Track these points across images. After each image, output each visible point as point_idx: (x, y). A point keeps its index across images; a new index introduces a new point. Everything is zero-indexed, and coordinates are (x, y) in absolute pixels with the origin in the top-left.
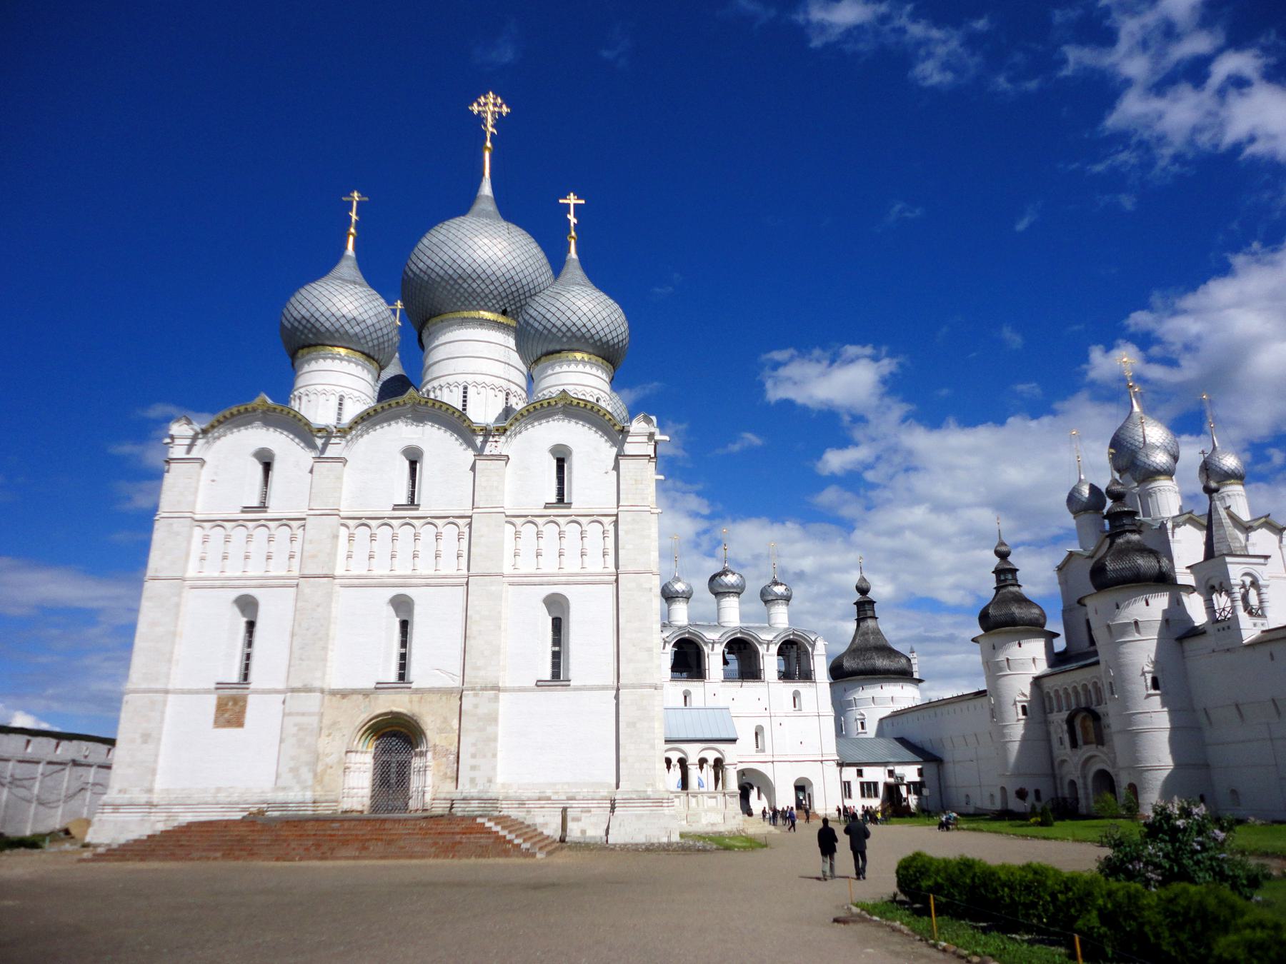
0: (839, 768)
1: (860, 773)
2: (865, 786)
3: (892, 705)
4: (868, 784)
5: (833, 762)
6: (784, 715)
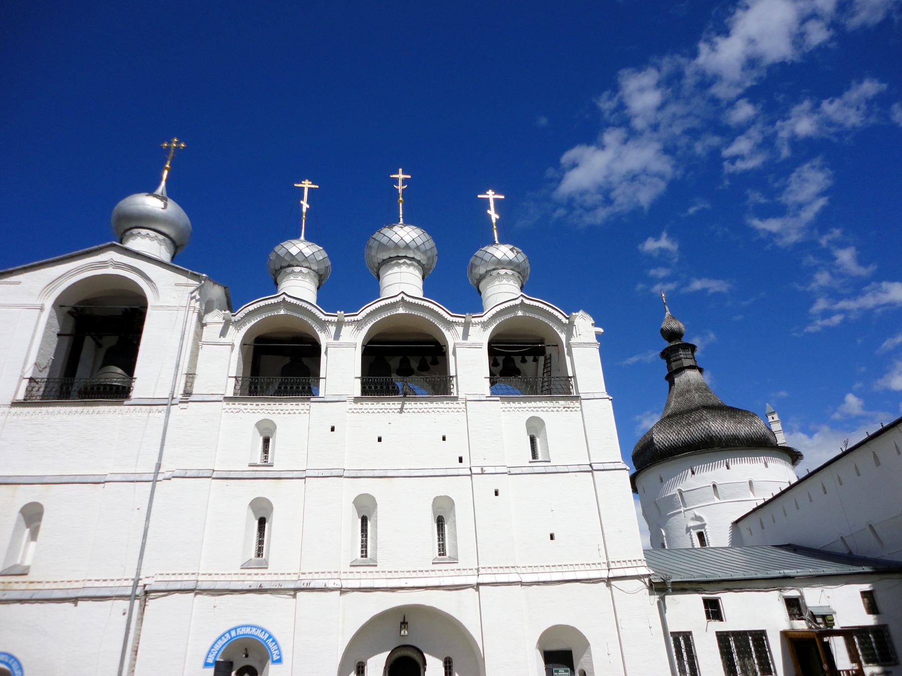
0: (656, 598)
1: (713, 610)
2: (732, 644)
3: (752, 497)
4: (741, 636)
5: (637, 582)
6: (505, 470)
